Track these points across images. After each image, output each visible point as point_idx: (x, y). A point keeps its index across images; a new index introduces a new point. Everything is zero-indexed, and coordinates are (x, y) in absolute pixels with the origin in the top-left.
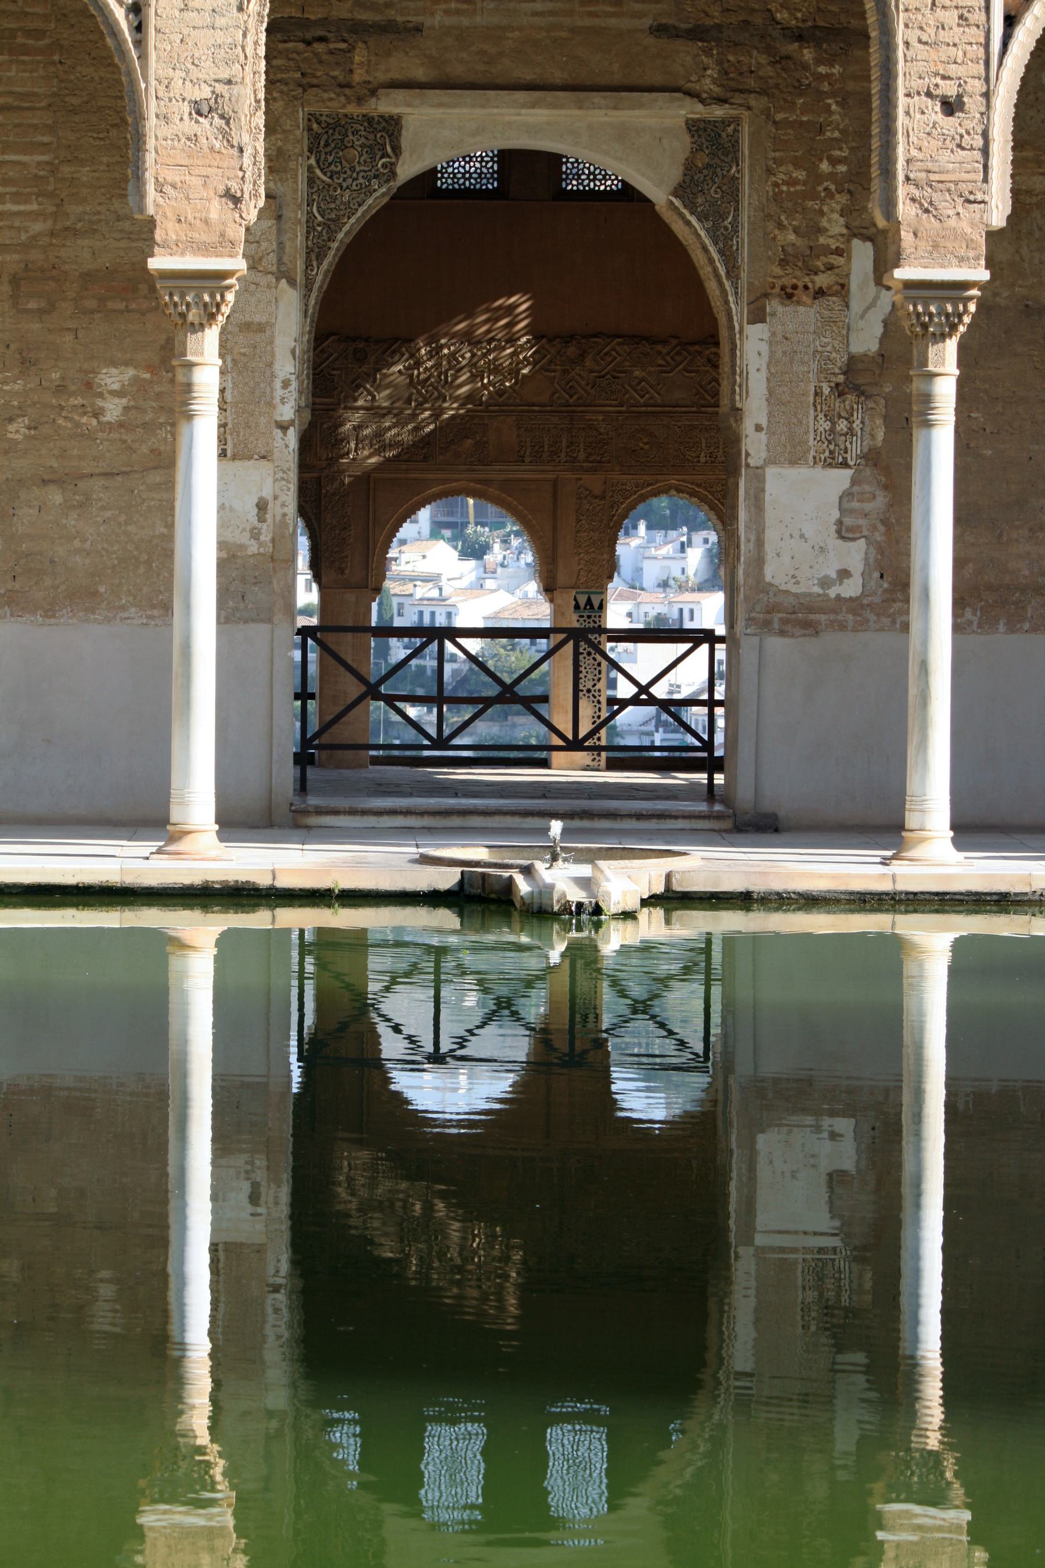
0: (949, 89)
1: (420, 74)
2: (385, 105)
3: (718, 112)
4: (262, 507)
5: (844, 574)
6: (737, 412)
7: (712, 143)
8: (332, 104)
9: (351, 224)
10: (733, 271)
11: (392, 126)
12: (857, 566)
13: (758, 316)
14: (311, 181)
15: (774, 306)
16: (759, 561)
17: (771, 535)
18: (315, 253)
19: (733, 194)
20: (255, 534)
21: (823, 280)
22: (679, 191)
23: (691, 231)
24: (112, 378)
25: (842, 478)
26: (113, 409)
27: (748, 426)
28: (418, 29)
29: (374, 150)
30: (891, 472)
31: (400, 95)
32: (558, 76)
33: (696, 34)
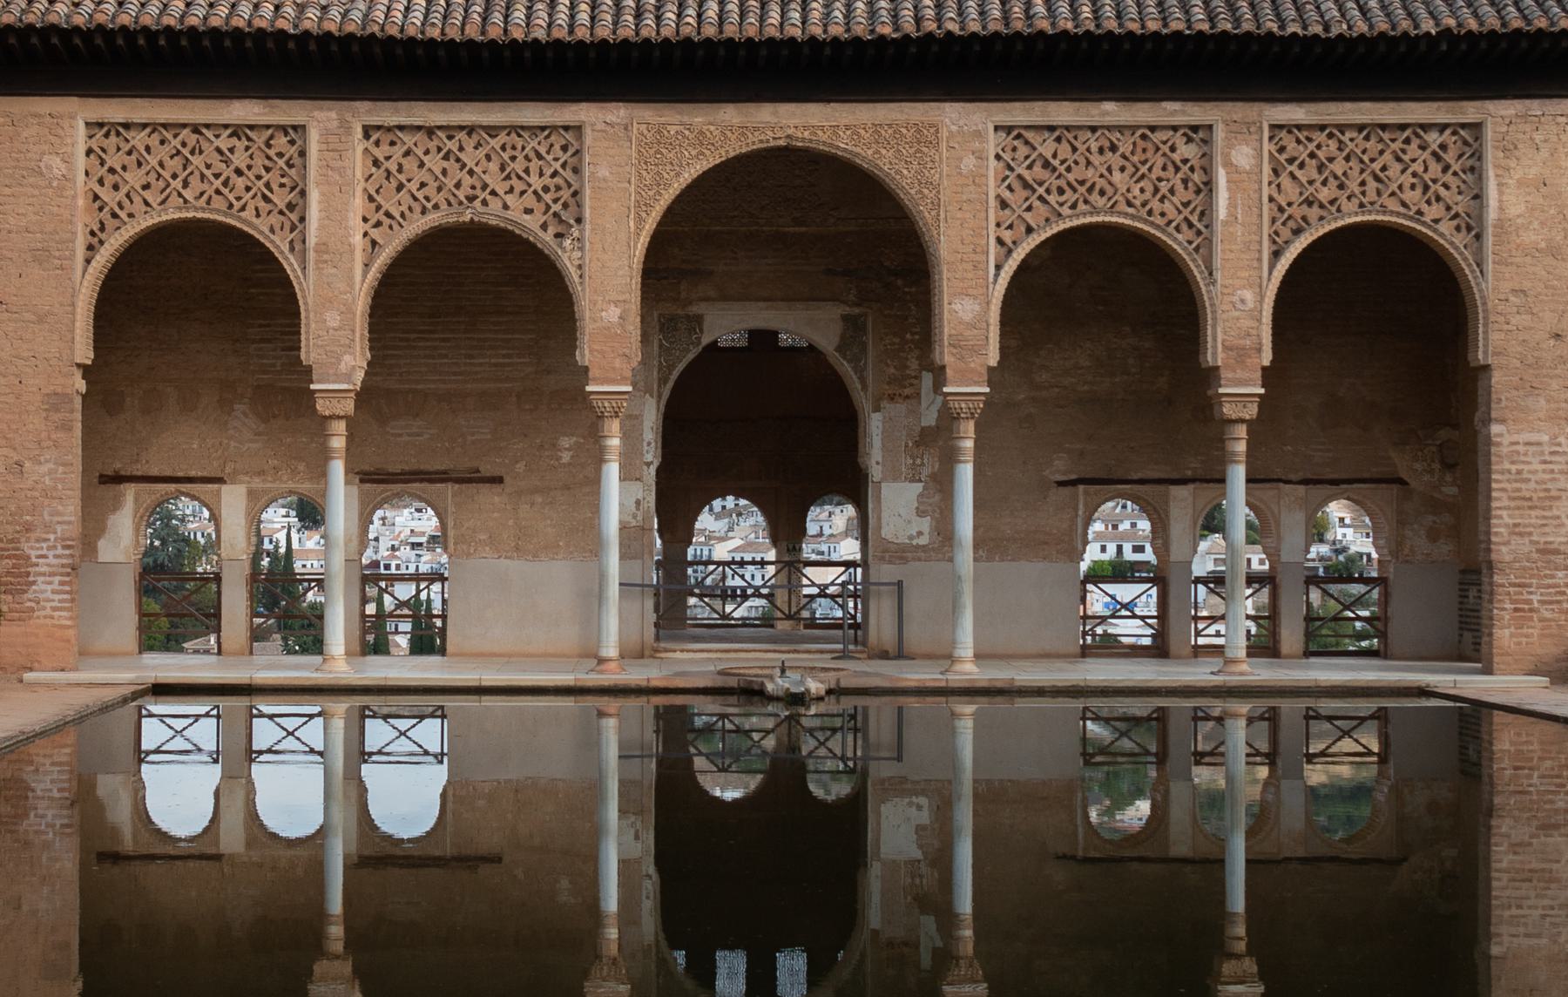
1: (712, 293)
2: (694, 309)
3: (857, 311)
4: (638, 503)
5: (920, 533)
9: (681, 367)
10: (865, 387)
11: (699, 319)
12: (926, 529)
13: (877, 409)
14: (661, 346)
16: (880, 528)
17: (885, 515)
18: (663, 381)
19: (864, 350)
20: (635, 517)
21: (907, 391)
22: (839, 349)
23: (845, 368)
24: (566, 442)
25: (919, 487)
26: (566, 457)
29: (691, 330)
30: (943, 484)
31: (703, 305)
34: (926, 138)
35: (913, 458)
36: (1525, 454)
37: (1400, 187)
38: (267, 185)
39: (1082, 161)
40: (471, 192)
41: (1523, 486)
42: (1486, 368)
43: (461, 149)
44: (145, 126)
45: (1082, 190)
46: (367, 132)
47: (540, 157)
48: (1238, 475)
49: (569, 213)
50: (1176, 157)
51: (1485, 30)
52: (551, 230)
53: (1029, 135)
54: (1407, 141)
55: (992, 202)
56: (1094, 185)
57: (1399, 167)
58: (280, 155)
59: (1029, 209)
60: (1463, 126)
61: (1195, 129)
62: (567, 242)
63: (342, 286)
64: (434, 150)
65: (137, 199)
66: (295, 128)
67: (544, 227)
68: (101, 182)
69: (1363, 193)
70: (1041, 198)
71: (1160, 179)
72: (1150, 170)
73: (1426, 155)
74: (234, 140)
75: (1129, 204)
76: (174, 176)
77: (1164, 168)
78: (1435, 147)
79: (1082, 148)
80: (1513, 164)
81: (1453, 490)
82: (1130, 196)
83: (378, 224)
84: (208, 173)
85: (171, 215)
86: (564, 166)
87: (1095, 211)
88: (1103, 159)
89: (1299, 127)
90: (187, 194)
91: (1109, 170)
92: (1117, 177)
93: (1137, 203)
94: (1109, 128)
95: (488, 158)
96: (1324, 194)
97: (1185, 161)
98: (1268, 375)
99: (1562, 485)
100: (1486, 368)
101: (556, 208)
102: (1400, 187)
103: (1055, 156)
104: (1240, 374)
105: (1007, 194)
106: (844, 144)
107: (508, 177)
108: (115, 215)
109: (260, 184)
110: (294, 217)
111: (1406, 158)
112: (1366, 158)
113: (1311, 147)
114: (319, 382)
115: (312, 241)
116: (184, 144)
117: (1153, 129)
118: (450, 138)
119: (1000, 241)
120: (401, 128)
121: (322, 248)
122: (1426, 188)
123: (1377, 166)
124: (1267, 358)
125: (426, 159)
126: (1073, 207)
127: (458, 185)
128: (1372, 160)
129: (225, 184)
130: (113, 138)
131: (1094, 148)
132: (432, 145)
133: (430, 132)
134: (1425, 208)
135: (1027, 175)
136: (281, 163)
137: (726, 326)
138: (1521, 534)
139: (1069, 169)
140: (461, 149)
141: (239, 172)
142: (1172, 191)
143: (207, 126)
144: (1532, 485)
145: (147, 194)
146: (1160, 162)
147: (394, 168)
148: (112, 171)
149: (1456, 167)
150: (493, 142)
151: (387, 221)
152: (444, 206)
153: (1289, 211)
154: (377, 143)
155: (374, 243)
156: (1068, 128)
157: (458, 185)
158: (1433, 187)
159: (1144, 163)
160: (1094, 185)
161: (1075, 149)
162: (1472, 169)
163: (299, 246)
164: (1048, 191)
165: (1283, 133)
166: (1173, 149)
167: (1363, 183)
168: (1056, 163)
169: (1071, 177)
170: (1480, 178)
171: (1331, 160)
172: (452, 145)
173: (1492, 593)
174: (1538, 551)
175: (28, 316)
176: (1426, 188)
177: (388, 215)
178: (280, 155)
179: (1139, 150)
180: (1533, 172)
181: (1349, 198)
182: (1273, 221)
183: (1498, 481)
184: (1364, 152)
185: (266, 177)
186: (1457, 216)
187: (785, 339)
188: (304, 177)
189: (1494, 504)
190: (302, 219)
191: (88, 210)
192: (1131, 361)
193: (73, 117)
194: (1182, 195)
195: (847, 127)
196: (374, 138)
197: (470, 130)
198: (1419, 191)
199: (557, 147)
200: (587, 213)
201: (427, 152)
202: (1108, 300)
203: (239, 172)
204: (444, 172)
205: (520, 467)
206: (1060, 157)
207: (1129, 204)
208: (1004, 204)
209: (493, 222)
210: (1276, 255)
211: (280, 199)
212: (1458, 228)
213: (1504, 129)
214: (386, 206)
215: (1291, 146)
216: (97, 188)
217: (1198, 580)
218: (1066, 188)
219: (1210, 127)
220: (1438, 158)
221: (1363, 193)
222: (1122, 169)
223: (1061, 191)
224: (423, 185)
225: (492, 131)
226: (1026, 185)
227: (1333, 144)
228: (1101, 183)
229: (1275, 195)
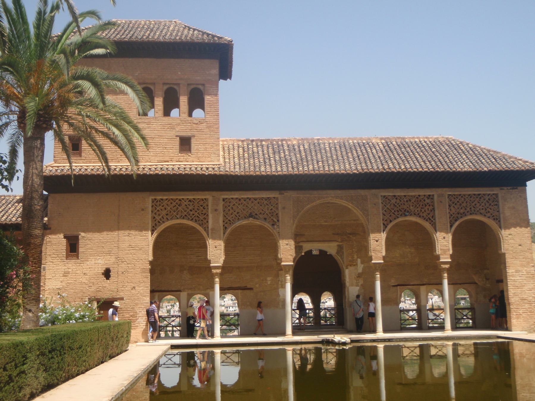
1: (305, 240)
3: (341, 244)
6: (345, 280)
7: (340, 248)
13: (347, 268)
15: (349, 267)
19: (343, 253)
21: (355, 264)
23: (338, 258)
24: (269, 279)
26: (269, 283)
27: (347, 282)
33: (337, 234)
35: (357, 280)
42: (504, 254)
44: (167, 199)
46: (224, 200)
50: (425, 202)
53: (389, 198)
54: (480, 198)
55: (381, 215)
57: (479, 204)
59: (390, 216)
60: (493, 194)
61: (429, 195)
62: (275, 226)
65: (165, 218)
66: (205, 199)
68: (155, 214)
73: (485, 201)
74: (189, 203)
76: (175, 211)
79: (402, 201)
81: (489, 285)
92: (411, 207)
96: (462, 211)
98: (452, 256)
100: (504, 254)
105: (385, 213)
108: (159, 222)
109: (196, 213)
110: (205, 221)
113: (458, 200)
114: (215, 263)
115: (210, 227)
117: (419, 196)
118: (245, 201)
119: (384, 224)
121: (212, 229)
122: (486, 209)
123: (473, 204)
124: (451, 252)
130: (158, 203)
132: (240, 203)
134: (486, 214)
136: (202, 208)
137: (315, 248)
141: (191, 211)
145: (167, 217)
148: (158, 211)
149: (492, 204)
151: (229, 222)
153: (453, 215)
155: (226, 228)
162: (496, 205)
163: (206, 229)
166: (424, 201)
167: (471, 208)
168: (396, 204)
169: (400, 208)
170: (498, 207)
171: (463, 203)
173: (510, 310)
175: (137, 249)
176: (486, 209)
177: (229, 220)
178: (202, 206)
182: (450, 218)
187: (315, 253)
188: (208, 211)
189: (509, 288)
190: (208, 222)
191: (152, 221)
192: (409, 255)
198: (484, 210)
200: (280, 219)
201: (239, 204)
205: (257, 286)
210: (451, 226)
214: (229, 218)
215: (453, 199)
217: (428, 310)
219: (433, 195)
220: (488, 202)
223: (398, 212)
224: (238, 213)
225: (255, 199)
227: (463, 199)
228: (407, 209)
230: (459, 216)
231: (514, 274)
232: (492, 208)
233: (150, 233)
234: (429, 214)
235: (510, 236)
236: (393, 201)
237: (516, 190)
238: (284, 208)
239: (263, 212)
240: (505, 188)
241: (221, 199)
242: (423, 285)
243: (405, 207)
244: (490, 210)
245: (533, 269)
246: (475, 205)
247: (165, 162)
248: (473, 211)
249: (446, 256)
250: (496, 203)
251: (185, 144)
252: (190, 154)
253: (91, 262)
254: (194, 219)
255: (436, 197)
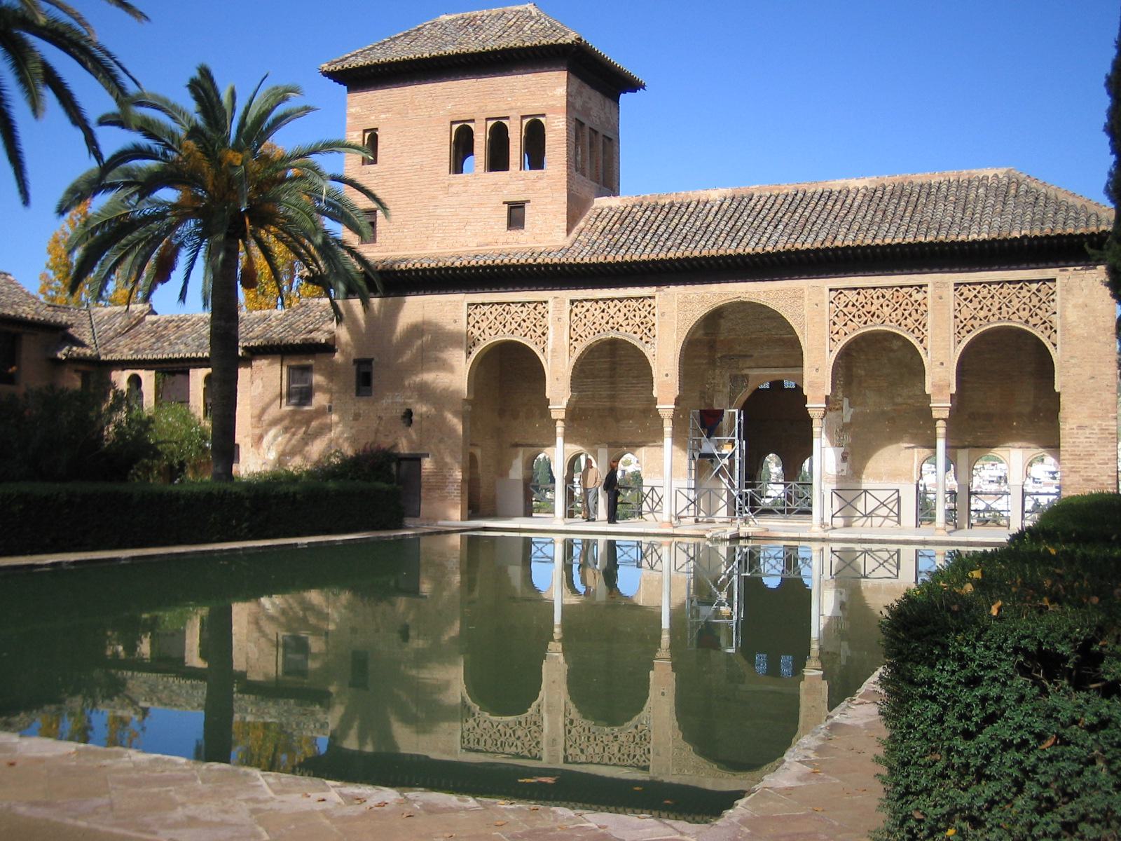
0: (817, 367)
8: (735, 372)
12: (845, 469)
28: (751, 356)
29: (743, 381)
32: (781, 365)
34: (798, 295)
36: (1078, 433)
37: (1018, 310)
38: (535, 325)
39: (869, 303)
40: (612, 325)
41: (1077, 449)
43: (609, 308)
45: (869, 315)
46: (572, 302)
47: (640, 310)
48: (941, 444)
49: (648, 330)
50: (912, 299)
51: (1043, 235)
52: (644, 341)
56: (874, 313)
57: (1017, 300)
58: (540, 313)
59: (846, 325)
61: (921, 286)
63: (561, 366)
64: (598, 309)
67: (641, 339)
69: (1000, 313)
70: (851, 320)
71: (905, 310)
72: (900, 305)
75: (891, 321)
77: (907, 304)
78: (1034, 290)
79: (869, 297)
80: (1070, 297)
82: (891, 318)
83: (576, 340)
84: (513, 322)
85: (498, 339)
86: (649, 313)
87: (875, 325)
88: (879, 301)
89: (970, 284)
90: (505, 330)
91: (881, 306)
92: (885, 308)
93: (894, 321)
94: (881, 288)
95: (619, 311)
96: (982, 314)
97: (916, 301)
99: (1096, 448)
100: (1059, 394)
101: (645, 331)
102: (1018, 310)
103: (857, 301)
104: (940, 398)
106: (762, 300)
107: (627, 319)
108: (479, 340)
110: (545, 338)
111: (1020, 296)
112: (1001, 297)
113: (975, 292)
116: (504, 310)
117: (901, 287)
120: (586, 300)
121: (553, 351)
124: (953, 390)
125: (595, 312)
126: (865, 323)
127: (607, 323)
128: (1004, 298)
129: (519, 325)
131: (875, 297)
132: (597, 307)
133: (597, 301)
134: (1030, 319)
135: (845, 310)
138: (1075, 472)
139: (863, 307)
140: (609, 308)
141: (524, 321)
142: (910, 315)
143: (513, 303)
144: (1080, 449)
145: (490, 331)
146: (905, 303)
147: (583, 317)
148: (478, 322)
150: (621, 304)
152: (602, 331)
153: (965, 322)
154: (577, 306)
156: (863, 289)
157: (607, 323)
158: (1033, 309)
159: (897, 303)
160: (874, 313)
161: (866, 298)
164: (854, 316)
165: (960, 288)
166: (911, 296)
167: (1000, 308)
168: (857, 304)
172: (603, 306)
174: (1083, 480)
178: (540, 313)
179: (895, 297)
180: (1080, 301)
181: (993, 315)
183: (1064, 447)
184: (1001, 294)
185: (534, 322)
186: (1045, 322)
193: (463, 301)
194: (915, 316)
195: (764, 292)
196: (575, 304)
197: (612, 300)
199: (647, 305)
201: (596, 310)
202: (878, 363)
203: (524, 321)
204: (602, 318)
206: (859, 301)
207: (891, 321)
208: (834, 324)
209: (620, 337)
211: (539, 332)
212: (1046, 328)
213: (1066, 281)
216: (472, 329)
218: (863, 315)
221: (1000, 313)
222: (888, 306)
223: (859, 316)
225: (621, 300)
226: (845, 315)
227: (986, 291)
229: (958, 315)
230: (976, 323)
231: (1075, 431)
232: (1044, 306)
233: (464, 355)
234: (916, 321)
235: (1073, 361)
236: (852, 296)
237: (1093, 271)
238: (663, 314)
239: (631, 322)
240: (1072, 268)
241: (568, 302)
242: (964, 447)
243: (873, 309)
244: (1038, 311)
245: (1114, 423)
246: (1010, 301)
247: (487, 245)
248: (1004, 314)
249: (943, 398)
250: (1052, 297)
251: (516, 214)
252: (522, 231)
253: (385, 402)
254: (528, 334)
255: (929, 289)
